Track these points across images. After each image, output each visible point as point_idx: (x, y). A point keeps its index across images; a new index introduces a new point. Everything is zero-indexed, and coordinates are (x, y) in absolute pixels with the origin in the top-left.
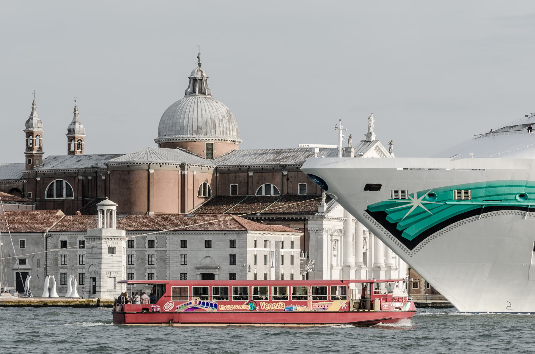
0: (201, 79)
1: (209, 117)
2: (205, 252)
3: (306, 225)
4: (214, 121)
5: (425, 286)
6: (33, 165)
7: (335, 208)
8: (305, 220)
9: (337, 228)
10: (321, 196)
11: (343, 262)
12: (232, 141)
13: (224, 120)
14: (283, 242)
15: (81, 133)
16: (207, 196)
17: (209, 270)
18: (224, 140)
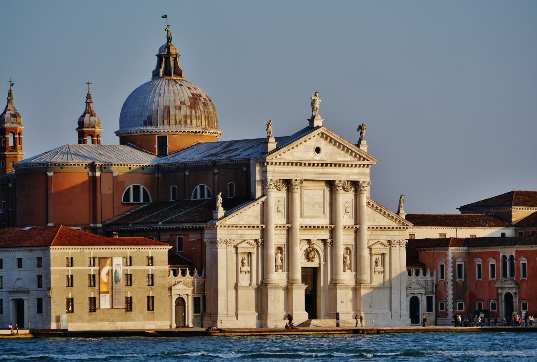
0: (167, 56)
1: (161, 104)
2: (16, 273)
3: (203, 236)
4: (168, 108)
5: (453, 308)
6: (5, 169)
7: (238, 212)
8: (202, 230)
9: (247, 237)
10: (215, 200)
11: (260, 279)
12: (192, 132)
13: (183, 107)
14: (130, 258)
15: (92, 126)
16: (142, 201)
17: (20, 295)
18: (180, 131)
